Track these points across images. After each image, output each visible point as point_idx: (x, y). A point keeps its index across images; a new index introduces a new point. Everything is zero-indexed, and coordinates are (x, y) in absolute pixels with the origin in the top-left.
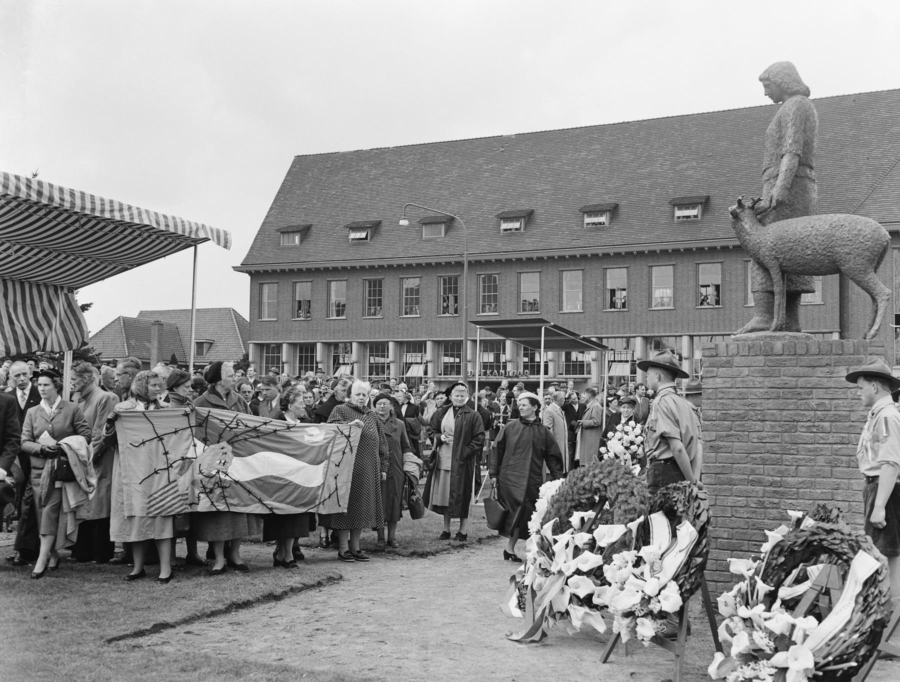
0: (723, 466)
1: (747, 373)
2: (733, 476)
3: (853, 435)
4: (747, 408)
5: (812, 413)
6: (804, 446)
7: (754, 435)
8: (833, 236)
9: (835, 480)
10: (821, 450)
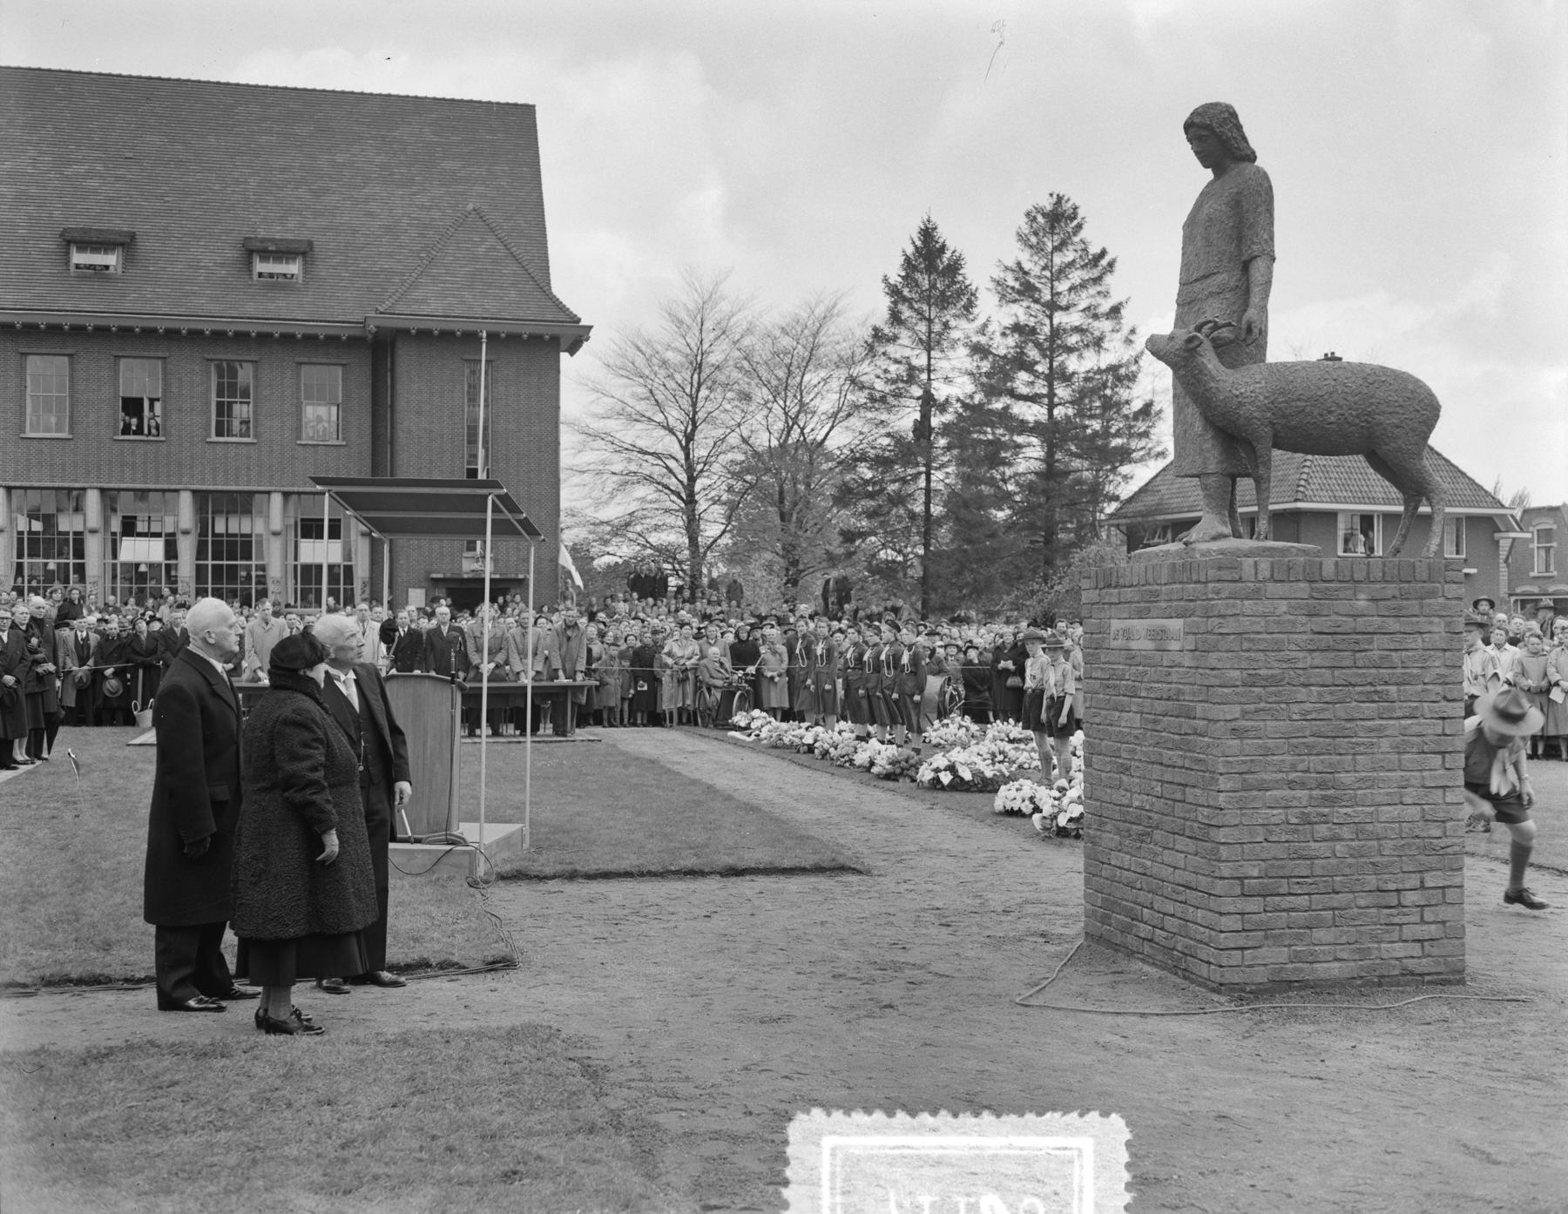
0: (1252, 761)
1: (1285, 609)
2: (1266, 776)
3: (1426, 704)
4: (1285, 666)
5: (1373, 671)
6: (1362, 723)
7: (1295, 708)
8: (1372, 397)
9: (1403, 774)
10: (1385, 728)
